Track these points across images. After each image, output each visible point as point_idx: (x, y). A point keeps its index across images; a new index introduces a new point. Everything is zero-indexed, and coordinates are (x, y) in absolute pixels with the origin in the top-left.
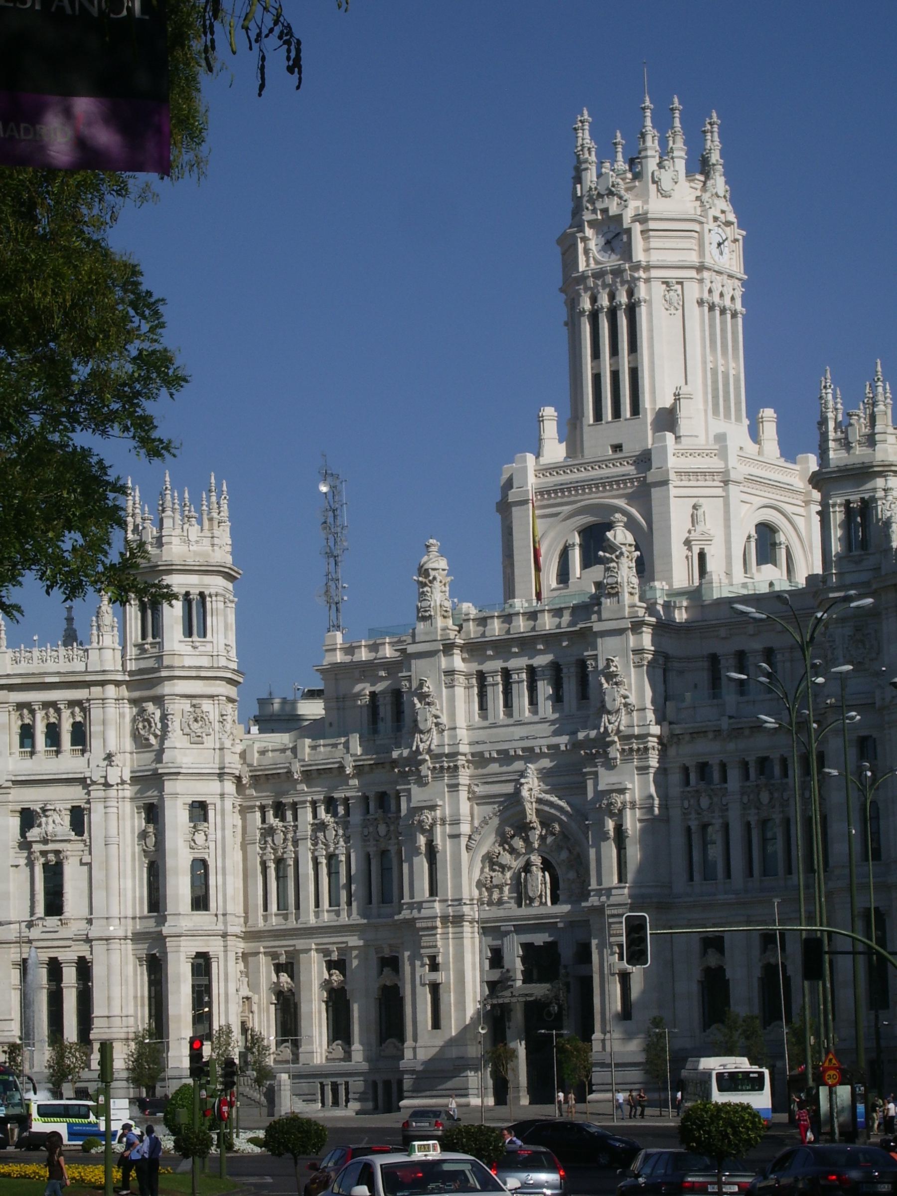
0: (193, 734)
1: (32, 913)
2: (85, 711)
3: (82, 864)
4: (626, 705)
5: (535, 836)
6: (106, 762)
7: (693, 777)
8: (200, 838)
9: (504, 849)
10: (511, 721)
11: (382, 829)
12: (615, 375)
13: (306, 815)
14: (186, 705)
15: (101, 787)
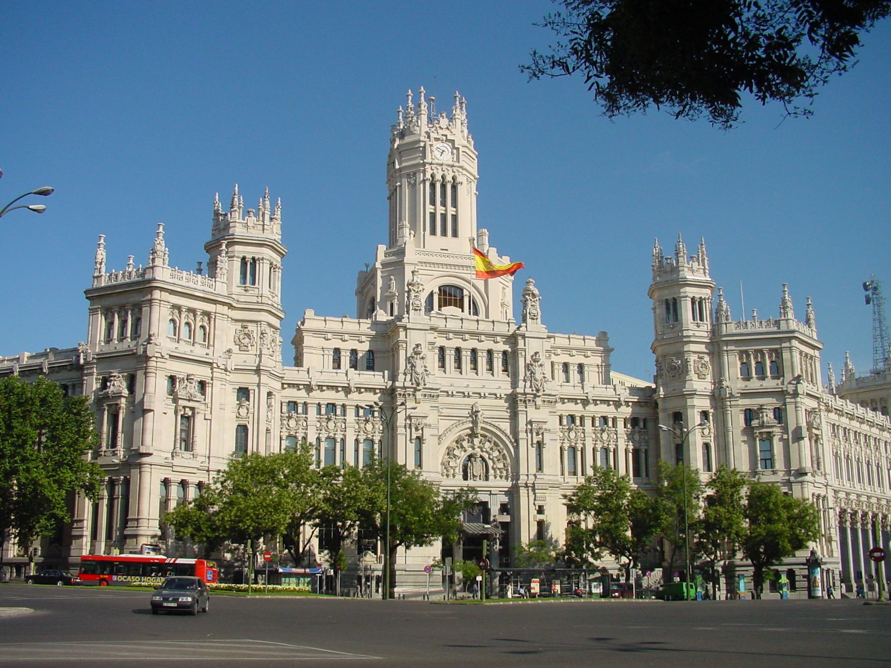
0: (271, 349)
1: (175, 448)
2: (209, 320)
3: (205, 419)
4: (544, 377)
5: (476, 441)
6: (223, 356)
7: (565, 422)
8: (269, 414)
9: (458, 447)
10: (461, 376)
11: (369, 427)
12: (444, 217)
13: (312, 411)
14: (269, 331)
15: (223, 371)
